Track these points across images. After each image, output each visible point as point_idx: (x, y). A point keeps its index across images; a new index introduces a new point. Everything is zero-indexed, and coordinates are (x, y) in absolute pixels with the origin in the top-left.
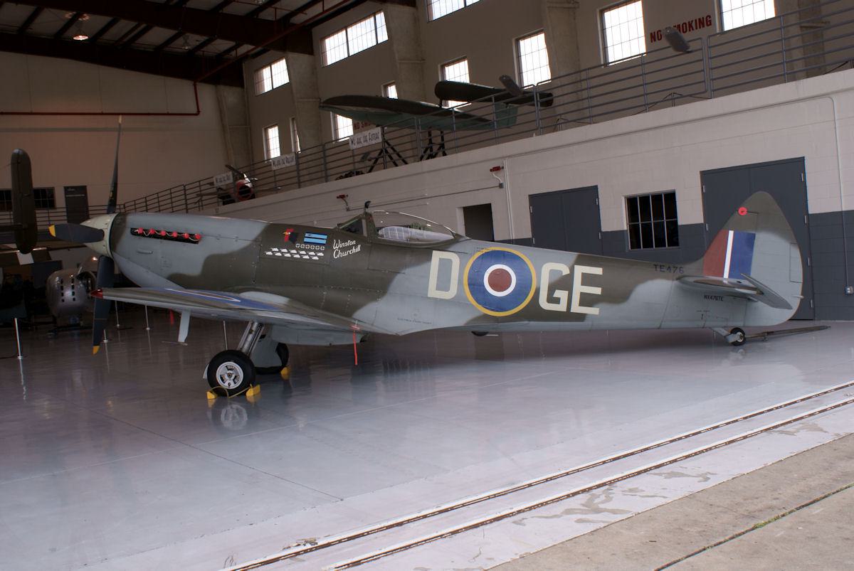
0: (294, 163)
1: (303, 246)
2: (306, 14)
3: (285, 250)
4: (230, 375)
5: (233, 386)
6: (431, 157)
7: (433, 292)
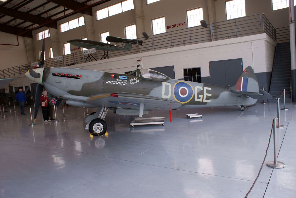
0: (62, 59)
1: (119, 80)
2: (56, 16)
3: (113, 82)
4: (98, 128)
5: (99, 132)
6: (105, 58)
7: (163, 96)
